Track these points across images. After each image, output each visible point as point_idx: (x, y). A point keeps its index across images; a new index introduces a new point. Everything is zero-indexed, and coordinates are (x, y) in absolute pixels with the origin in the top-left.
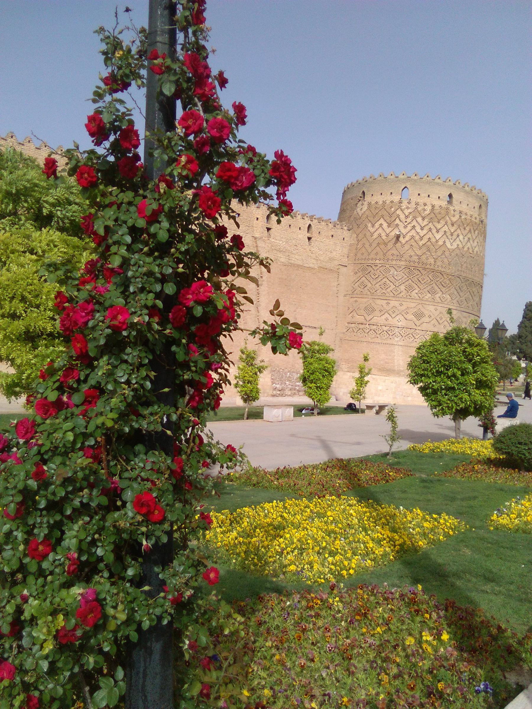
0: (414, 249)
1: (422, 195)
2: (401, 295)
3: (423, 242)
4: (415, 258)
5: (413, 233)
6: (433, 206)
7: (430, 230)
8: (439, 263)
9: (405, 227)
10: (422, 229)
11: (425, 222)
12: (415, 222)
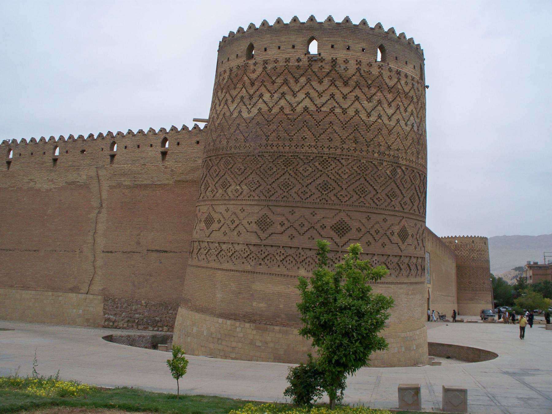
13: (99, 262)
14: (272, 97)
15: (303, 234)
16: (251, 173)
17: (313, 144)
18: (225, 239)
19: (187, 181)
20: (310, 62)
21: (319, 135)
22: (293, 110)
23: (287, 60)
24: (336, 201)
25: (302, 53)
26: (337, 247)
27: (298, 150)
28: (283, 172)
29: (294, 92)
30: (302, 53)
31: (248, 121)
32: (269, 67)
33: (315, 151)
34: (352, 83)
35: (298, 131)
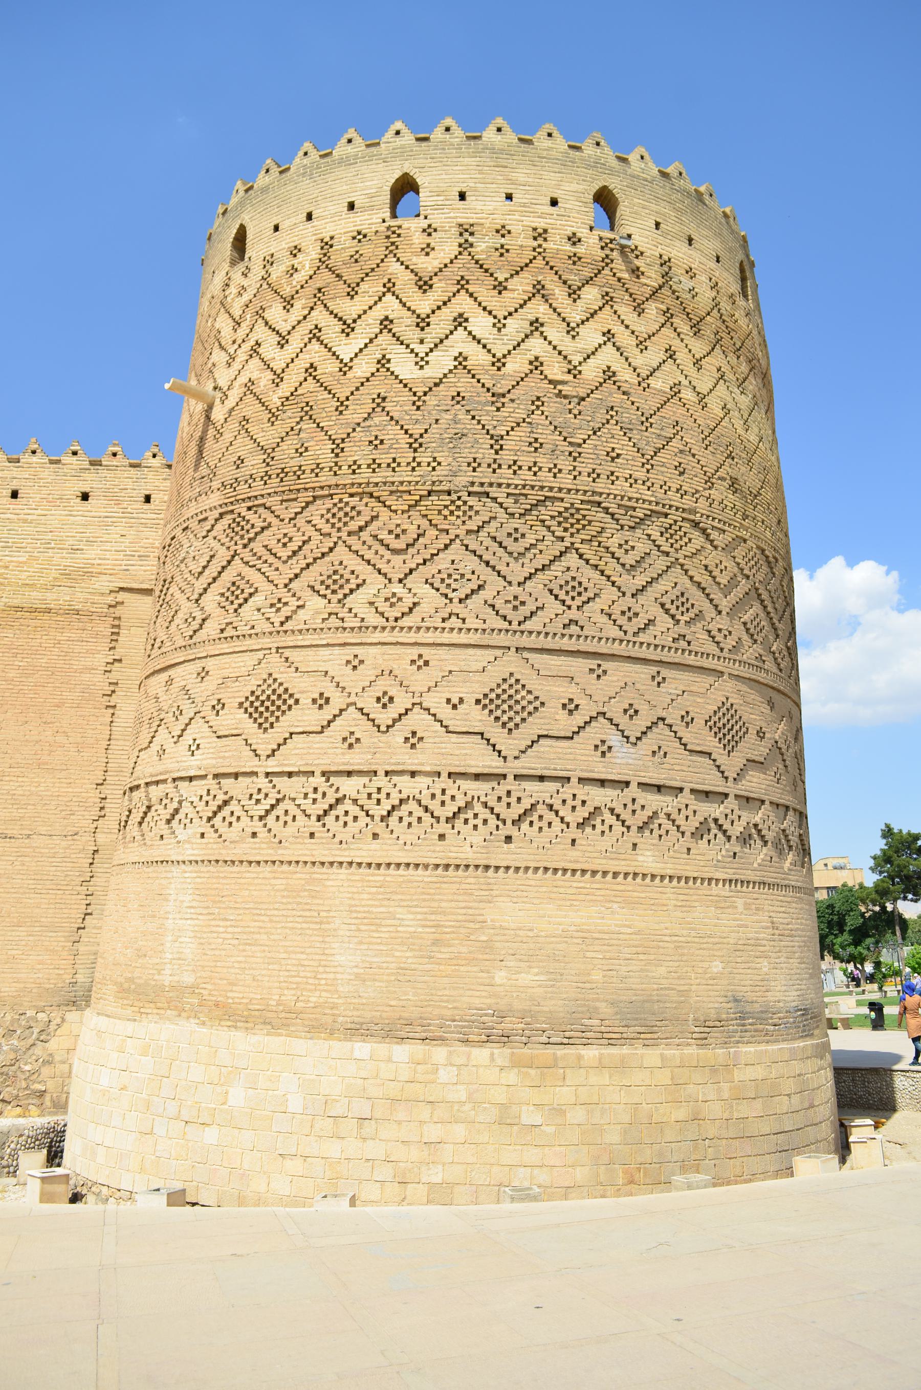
3: (285, 389)
6: (326, 245)
7: (316, 335)
8: (359, 452)
15: (638, 739)
16: (446, 547)
17: (641, 474)
18: (356, 759)
20: (608, 252)
21: (653, 454)
22: (574, 371)
23: (541, 234)
25: (582, 223)
26: (721, 782)
28: (561, 546)
29: (568, 325)
30: (582, 223)
31: (420, 391)
33: (648, 495)
34: (708, 332)
35: (595, 433)
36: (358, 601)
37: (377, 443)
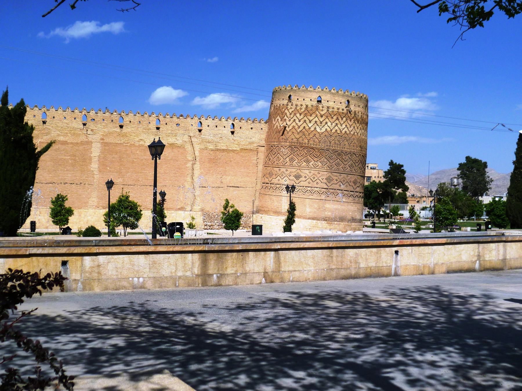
0: (295, 135)
1: (300, 99)
2: (287, 164)
3: (300, 129)
4: (295, 140)
5: (294, 124)
6: (307, 106)
7: (305, 121)
8: (311, 142)
9: (290, 120)
10: (300, 121)
11: (302, 116)
12: (295, 118)
13: (197, 193)
14: (332, 124)
18: (310, 185)
19: (247, 149)
22: (341, 132)
23: (338, 109)
24: (355, 172)
27: (343, 150)
28: (337, 158)
31: (320, 134)
32: (331, 110)
36: (311, 164)
37: (314, 141)
